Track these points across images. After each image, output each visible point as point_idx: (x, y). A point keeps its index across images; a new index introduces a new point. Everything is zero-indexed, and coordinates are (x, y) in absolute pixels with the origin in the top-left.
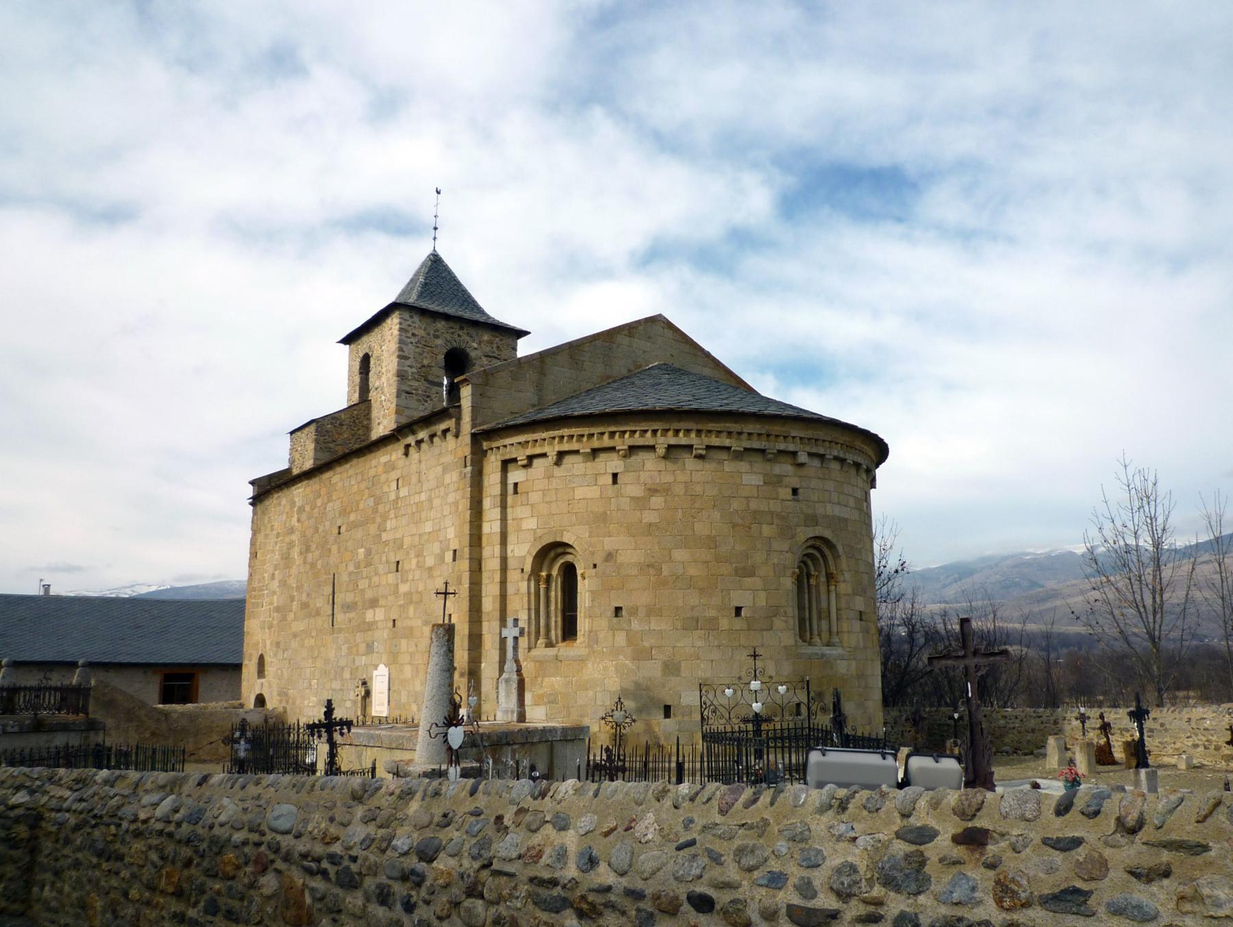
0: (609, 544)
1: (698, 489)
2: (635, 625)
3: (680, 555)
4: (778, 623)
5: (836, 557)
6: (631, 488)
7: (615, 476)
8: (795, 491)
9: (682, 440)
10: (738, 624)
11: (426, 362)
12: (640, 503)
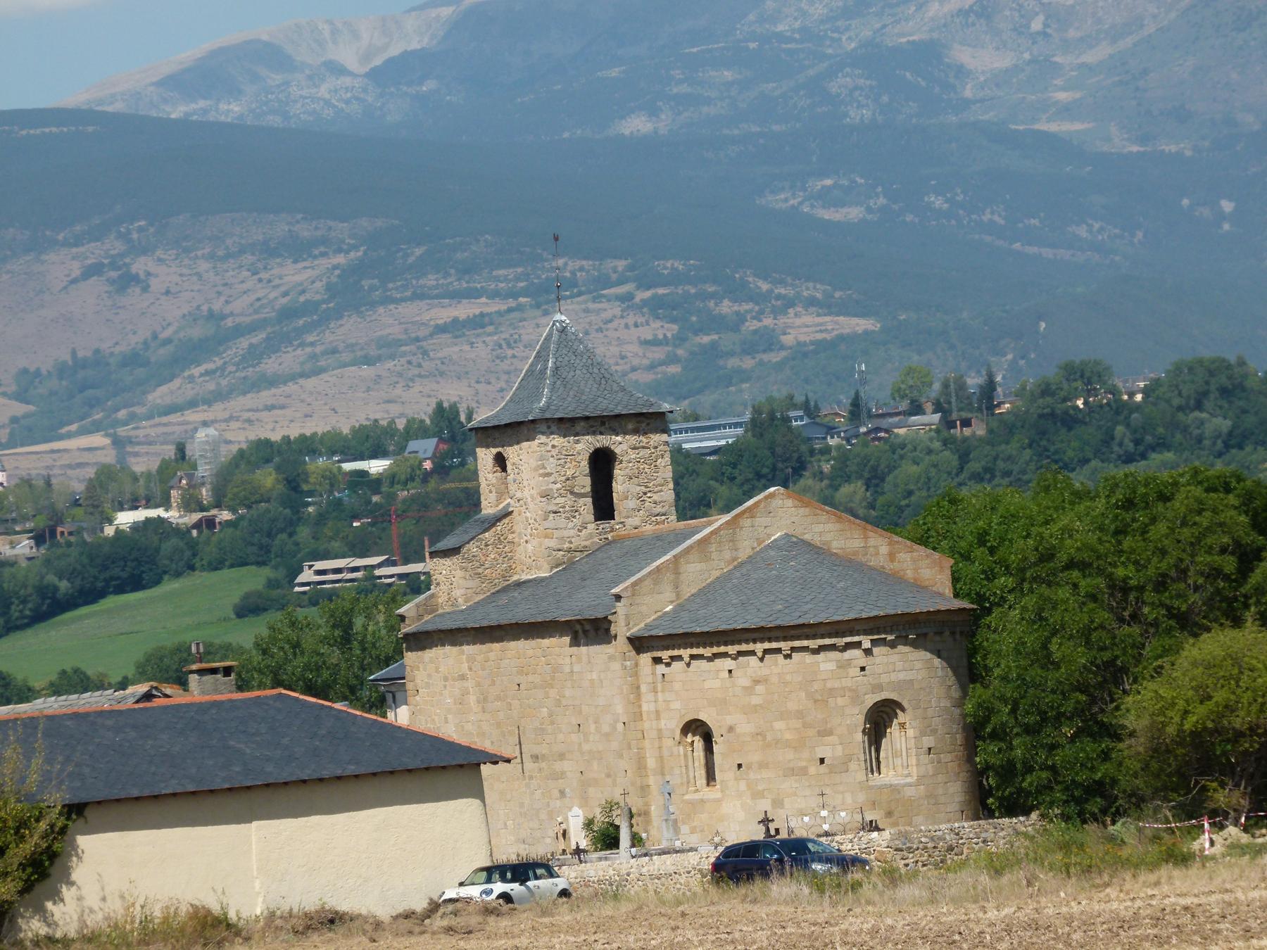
0: (729, 720)
1: (788, 678)
2: (752, 776)
3: (779, 725)
4: (853, 766)
6: (742, 680)
7: (730, 671)
8: (863, 669)
9: (774, 645)
10: (823, 768)
11: (569, 473)
12: (749, 690)
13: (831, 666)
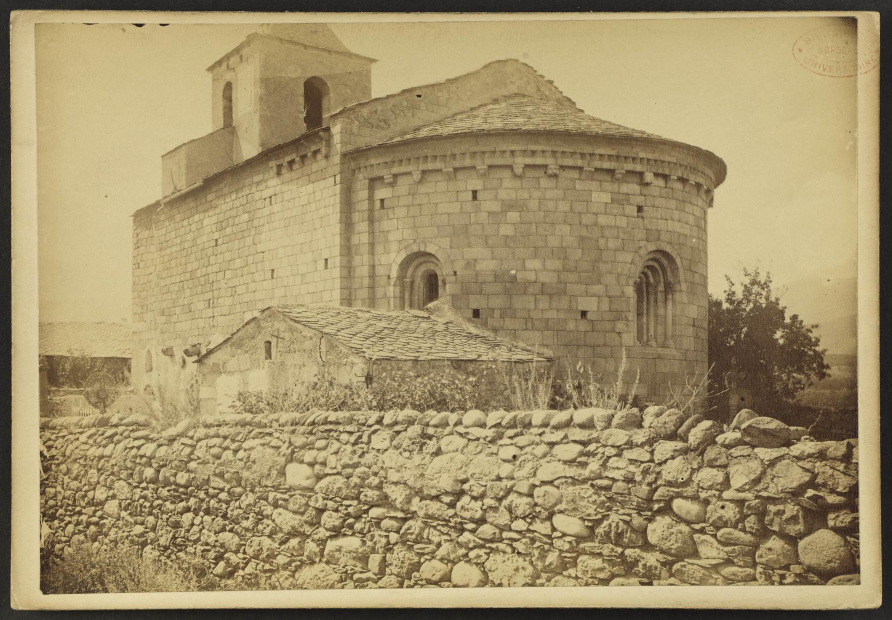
3: (534, 264)
5: (675, 270)
7: (475, 193)
8: (640, 209)
10: (583, 326)
13: (606, 197)
